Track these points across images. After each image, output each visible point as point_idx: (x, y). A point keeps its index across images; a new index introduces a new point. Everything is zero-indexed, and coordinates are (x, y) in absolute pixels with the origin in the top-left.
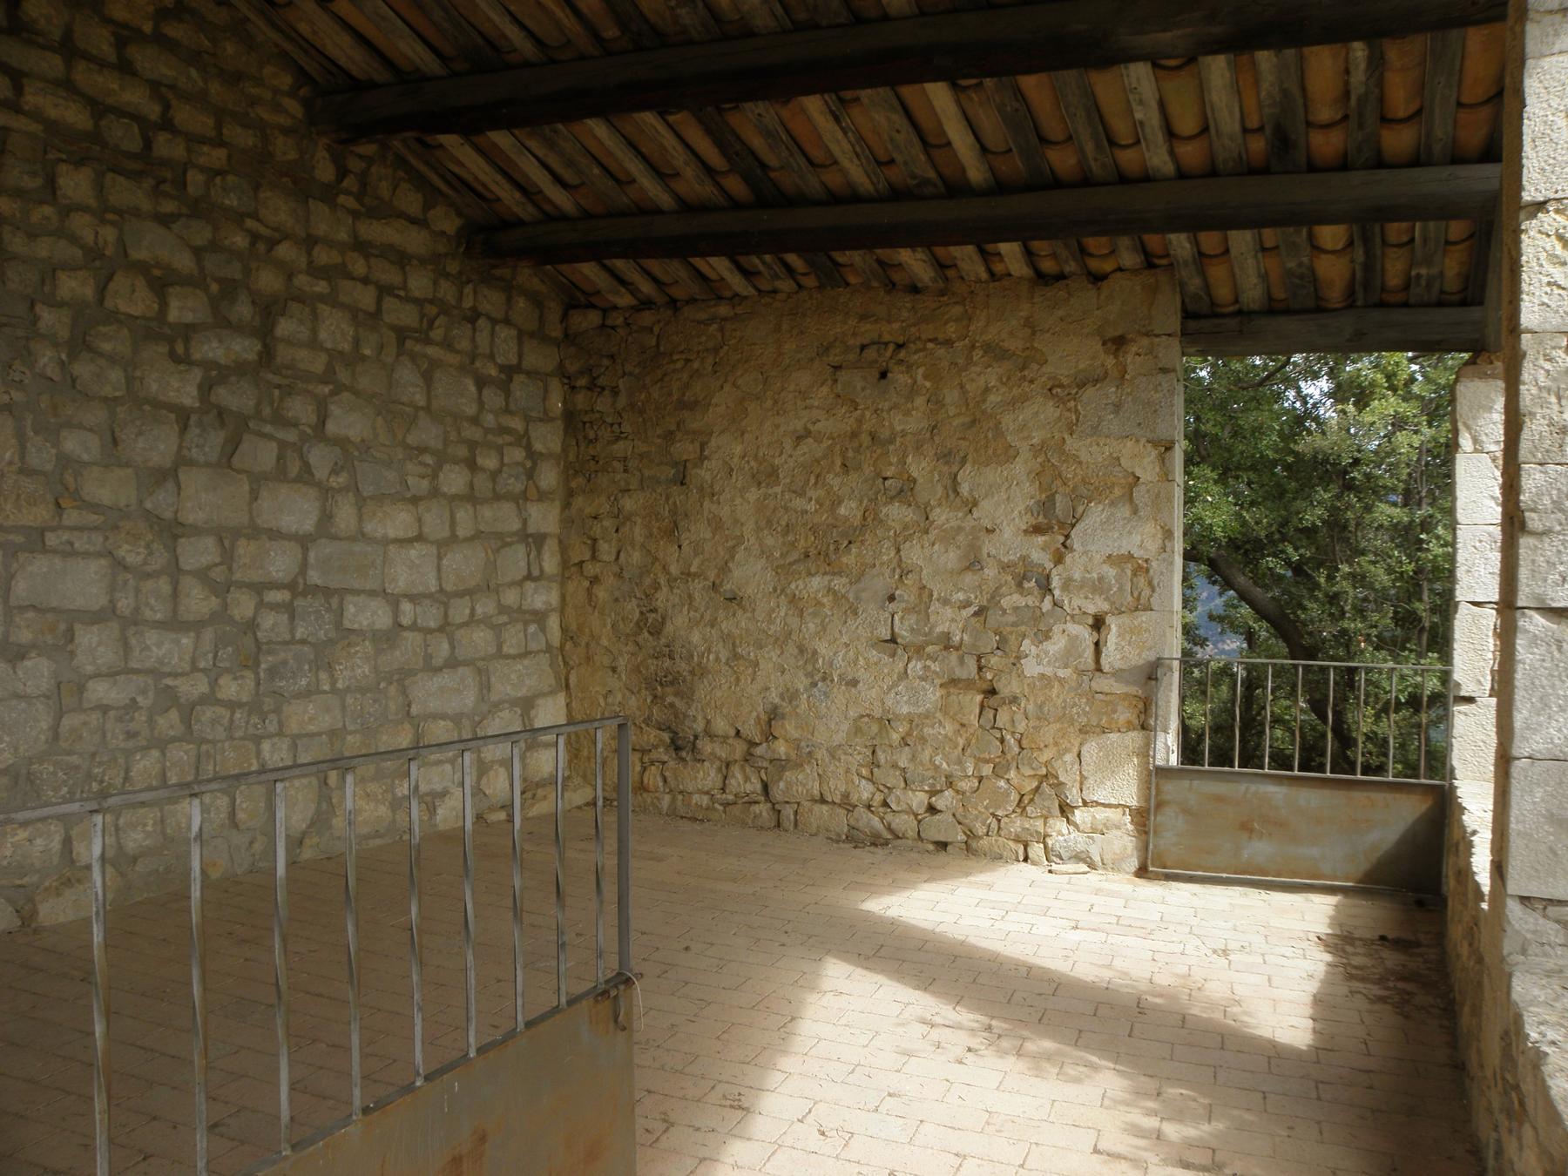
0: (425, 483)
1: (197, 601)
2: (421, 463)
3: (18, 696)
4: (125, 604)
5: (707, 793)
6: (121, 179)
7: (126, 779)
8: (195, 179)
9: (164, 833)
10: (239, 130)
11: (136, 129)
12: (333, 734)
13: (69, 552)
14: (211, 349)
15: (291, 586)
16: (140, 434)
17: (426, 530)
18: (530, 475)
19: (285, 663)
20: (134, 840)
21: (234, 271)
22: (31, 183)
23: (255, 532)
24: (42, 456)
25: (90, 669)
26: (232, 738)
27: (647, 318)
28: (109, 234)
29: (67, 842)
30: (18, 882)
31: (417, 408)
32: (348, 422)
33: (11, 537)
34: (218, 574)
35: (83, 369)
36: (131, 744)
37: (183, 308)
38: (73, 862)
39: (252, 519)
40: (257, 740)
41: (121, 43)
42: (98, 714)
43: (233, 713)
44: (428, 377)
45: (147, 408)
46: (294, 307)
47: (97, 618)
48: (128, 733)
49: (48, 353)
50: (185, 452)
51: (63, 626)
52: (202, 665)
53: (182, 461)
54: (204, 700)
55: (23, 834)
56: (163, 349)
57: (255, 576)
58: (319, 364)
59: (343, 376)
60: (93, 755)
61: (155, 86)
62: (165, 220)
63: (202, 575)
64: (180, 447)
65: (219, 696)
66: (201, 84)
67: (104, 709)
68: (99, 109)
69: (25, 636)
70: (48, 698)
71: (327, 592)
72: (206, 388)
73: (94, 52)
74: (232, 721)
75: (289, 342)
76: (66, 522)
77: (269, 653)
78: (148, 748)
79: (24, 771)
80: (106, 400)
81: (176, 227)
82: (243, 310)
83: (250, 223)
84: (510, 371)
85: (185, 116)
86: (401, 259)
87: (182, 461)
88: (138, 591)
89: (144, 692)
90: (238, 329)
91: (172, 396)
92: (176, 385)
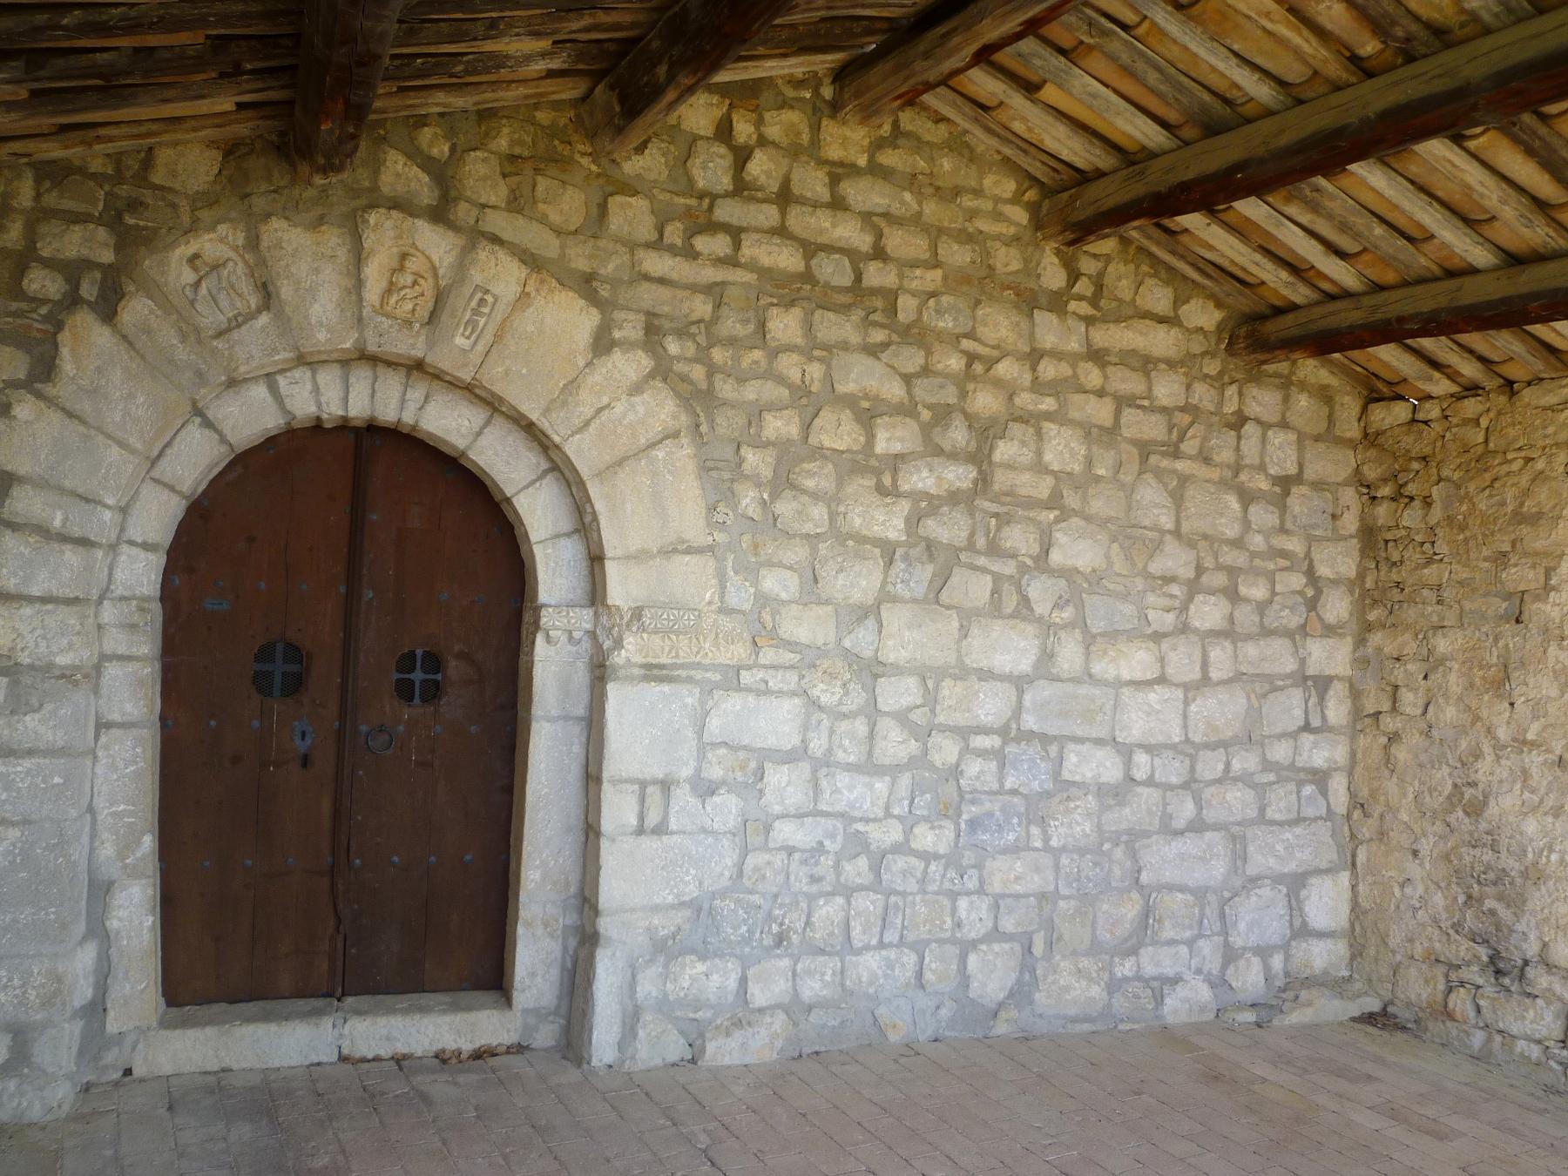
0: (1170, 618)
1: (895, 744)
2: (1165, 594)
3: (704, 830)
4: (818, 745)
5: (1539, 1042)
6: (831, 315)
7: (807, 923)
8: (907, 307)
9: (843, 985)
10: (956, 247)
11: (847, 262)
12: (1042, 897)
13: (764, 691)
14: (921, 479)
15: (1003, 732)
16: (841, 570)
17: (1170, 671)
18: (1312, 605)
19: (990, 815)
20: (811, 989)
21: (950, 395)
22: (741, 330)
23: (962, 672)
24: (740, 595)
25: (777, 809)
26: (924, 892)
27: (1471, 406)
28: (816, 371)
29: (743, 980)
30: (692, 1015)
31: (1163, 532)
32: (1077, 550)
33: (708, 675)
34: (918, 716)
35: (785, 507)
36: (814, 889)
37: (890, 439)
38: (746, 1002)
39: (960, 658)
40: (954, 896)
41: (834, 180)
42: (784, 855)
43: (927, 867)
44: (1178, 498)
45: (850, 543)
46: (1016, 429)
47: (788, 758)
48: (811, 876)
49: (751, 494)
50: (890, 588)
51: (753, 764)
52: (896, 811)
53: (885, 597)
54: (897, 849)
55: (700, 968)
56: (870, 482)
57: (960, 719)
58: (1044, 488)
59: (1071, 500)
60: (776, 896)
61: (867, 217)
62: (873, 351)
63: (902, 717)
64: (884, 583)
65: (913, 846)
66: (916, 207)
67: (790, 851)
68: (811, 250)
69: (715, 772)
70: (734, 835)
71: (1045, 739)
72: (914, 521)
73: (809, 195)
74: (925, 872)
75: (1009, 466)
76: (762, 661)
77: (973, 802)
78: (832, 894)
79: (706, 906)
80: (807, 536)
81: (884, 356)
82: (958, 435)
83: (966, 344)
84: (1286, 483)
85: (899, 242)
86: (1146, 364)
87: (885, 597)
88: (832, 732)
89: (832, 836)
90: (953, 456)
91: (877, 531)
92: (882, 519)
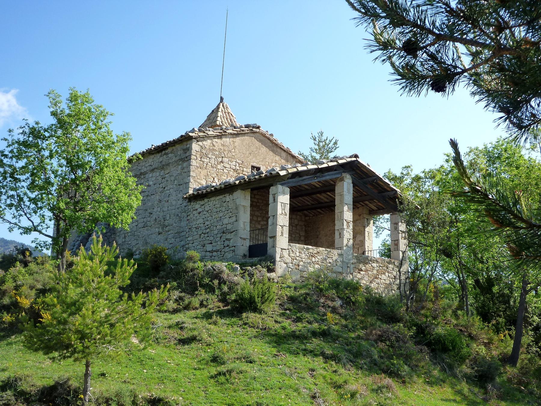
8: (260, 207)
14: (262, 223)
18: (300, 238)
27: (314, 217)
37: (259, 219)
62: (258, 211)
72: (261, 227)
82: (265, 219)
84: (297, 225)
85: (260, 201)
